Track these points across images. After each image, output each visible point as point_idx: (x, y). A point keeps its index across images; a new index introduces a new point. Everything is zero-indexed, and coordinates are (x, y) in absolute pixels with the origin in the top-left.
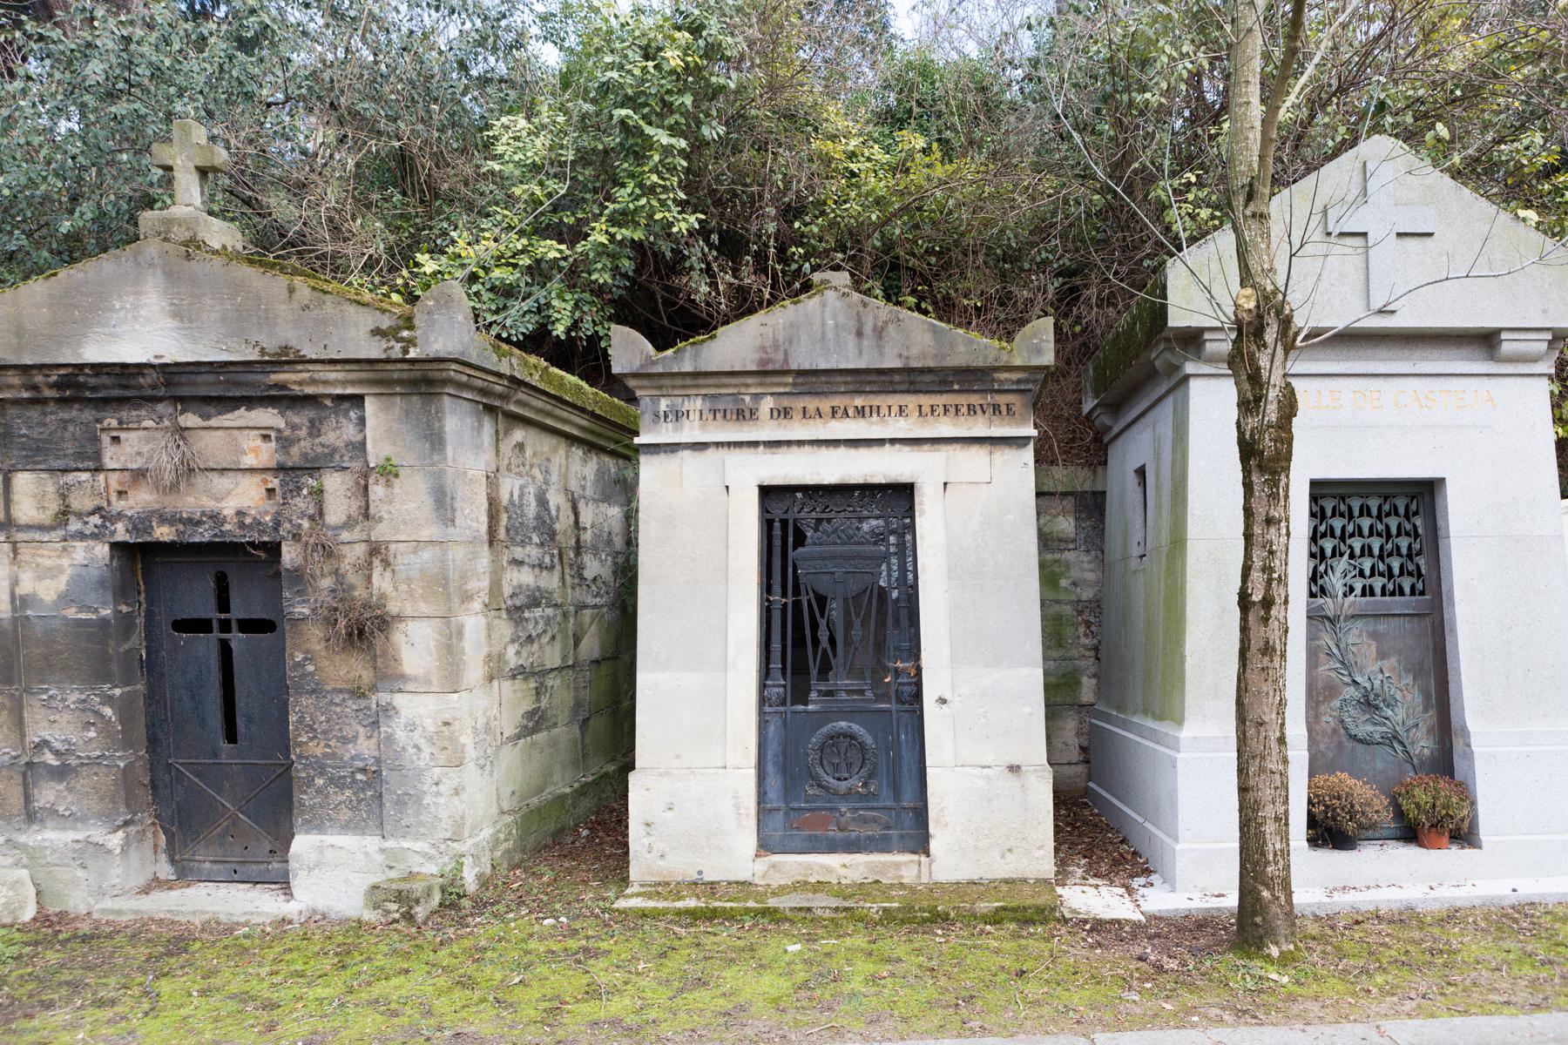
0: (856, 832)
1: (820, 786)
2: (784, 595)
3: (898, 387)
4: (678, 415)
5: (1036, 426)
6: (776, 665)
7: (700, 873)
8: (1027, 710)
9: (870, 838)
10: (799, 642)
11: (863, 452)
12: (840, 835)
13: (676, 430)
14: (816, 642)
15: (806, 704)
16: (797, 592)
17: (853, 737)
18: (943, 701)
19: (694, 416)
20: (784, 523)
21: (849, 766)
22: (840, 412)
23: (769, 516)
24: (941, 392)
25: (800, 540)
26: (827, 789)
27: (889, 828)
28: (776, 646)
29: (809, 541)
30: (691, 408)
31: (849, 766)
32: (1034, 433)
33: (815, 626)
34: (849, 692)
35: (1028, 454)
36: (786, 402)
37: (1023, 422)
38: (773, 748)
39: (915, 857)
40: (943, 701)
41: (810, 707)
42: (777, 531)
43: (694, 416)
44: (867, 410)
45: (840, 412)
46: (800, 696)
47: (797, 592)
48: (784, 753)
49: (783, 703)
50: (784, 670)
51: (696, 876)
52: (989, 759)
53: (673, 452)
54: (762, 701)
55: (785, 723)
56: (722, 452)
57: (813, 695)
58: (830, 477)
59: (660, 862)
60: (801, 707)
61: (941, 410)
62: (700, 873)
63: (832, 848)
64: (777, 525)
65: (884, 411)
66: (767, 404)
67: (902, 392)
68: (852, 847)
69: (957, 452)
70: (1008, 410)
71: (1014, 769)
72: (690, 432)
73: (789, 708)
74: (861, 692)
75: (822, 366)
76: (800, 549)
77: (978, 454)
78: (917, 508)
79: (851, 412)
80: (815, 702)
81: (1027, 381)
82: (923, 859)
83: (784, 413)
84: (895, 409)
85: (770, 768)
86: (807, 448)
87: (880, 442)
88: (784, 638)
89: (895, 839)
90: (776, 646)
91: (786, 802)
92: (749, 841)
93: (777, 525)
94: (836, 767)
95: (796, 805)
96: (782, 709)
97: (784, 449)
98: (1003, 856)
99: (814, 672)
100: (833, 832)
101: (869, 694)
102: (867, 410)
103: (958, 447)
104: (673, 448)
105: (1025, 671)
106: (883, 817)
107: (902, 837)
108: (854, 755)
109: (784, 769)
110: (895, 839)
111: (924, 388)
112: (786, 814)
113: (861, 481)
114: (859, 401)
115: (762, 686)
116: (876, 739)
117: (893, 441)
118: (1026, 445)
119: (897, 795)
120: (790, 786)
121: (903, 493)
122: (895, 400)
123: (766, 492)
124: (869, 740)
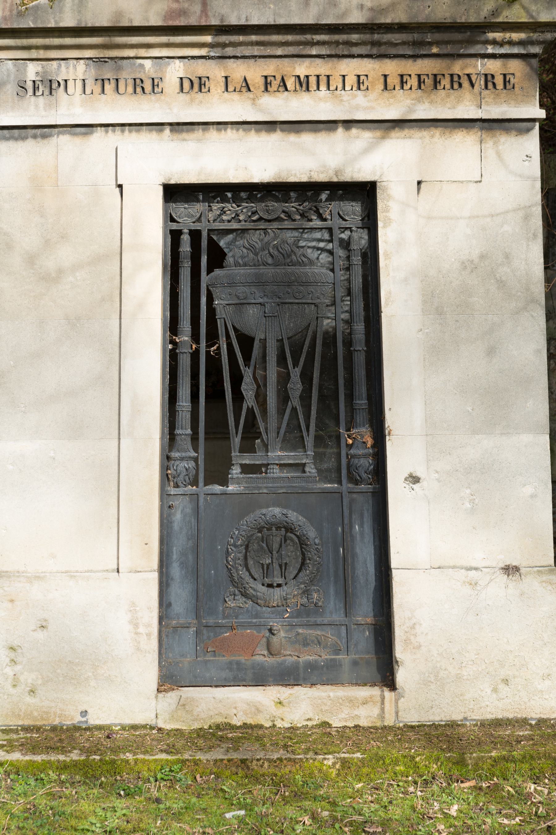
0: (290, 656)
1: (245, 595)
2: (195, 337)
3: (356, 50)
4: (50, 86)
5: (542, 106)
6: (184, 430)
7: (84, 713)
8: (529, 490)
9: (312, 666)
10: (215, 394)
11: (307, 139)
12: (270, 660)
13: (48, 106)
14: (238, 397)
15: (224, 482)
16: (212, 337)
17: (289, 529)
18: (414, 479)
19: (75, 88)
20: (195, 235)
21: (284, 567)
22: (275, 84)
23: (174, 226)
24: (415, 57)
25: (217, 258)
26: (254, 599)
27: (337, 651)
28: (184, 403)
29: (229, 259)
30: (71, 77)
31: (284, 567)
32: (542, 114)
33: (237, 379)
34: (281, 465)
35: (531, 144)
36: (202, 68)
37: (525, 99)
38: (180, 543)
39: (375, 692)
40: (414, 479)
41: (231, 488)
42: (186, 247)
43: (75, 88)
44: (313, 80)
45: (275, 84)
46: (217, 473)
47: (212, 337)
48: (197, 547)
49: (195, 483)
50: (194, 438)
51: (78, 719)
52: (477, 557)
53: (44, 137)
54: (166, 477)
55: (197, 510)
56: (114, 138)
57: (236, 471)
58: (260, 172)
59: (29, 699)
60: (217, 488)
61: (414, 82)
62: (84, 713)
63: (259, 678)
64: (186, 238)
65: (336, 82)
66: (175, 71)
67: (361, 56)
68: (289, 677)
69: (436, 139)
70: (506, 82)
71: (510, 570)
72: (71, 108)
73: (203, 489)
74: (301, 467)
75: (255, 21)
76: (217, 272)
77: (465, 143)
78: (381, 215)
79: (290, 83)
80: (238, 482)
81: (532, 43)
82: (387, 694)
83: (200, 84)
84: (351, 80)
85: (176, 571)
86: (230, 133)
87: (330, 125)
88: (195, 396)
89: (346, 667)
90: (184, 403)
91: (198, 616)
92: (151, 674)
93: (186, 238)
94: (267, 570)
95: (211, 621)
96: (191, 489)
97: (199, 133)
98: (495, 690)
99: (236, 441)
100: (261, 657)
101: (311, 470)
102: (313, 80)
103: (437, 132)
104: (44, 130)
105: (526, 438)
106: (329, 635)
107: (355, 663)
108: (290, 553)
109: (195, 573)
110: (346, 667)
111: (393, 51)
112: (198, 633)
113: (304, 179)
114: (302, 68)
115: (166, 459)
116: (320, 531)
117: (348, 124)
118: (528, 130)
119: (348, 606)
120: (203, 602)
121: (365, 193)
122: (350, 68)
123: (174, 193)
124: (311, 533)
